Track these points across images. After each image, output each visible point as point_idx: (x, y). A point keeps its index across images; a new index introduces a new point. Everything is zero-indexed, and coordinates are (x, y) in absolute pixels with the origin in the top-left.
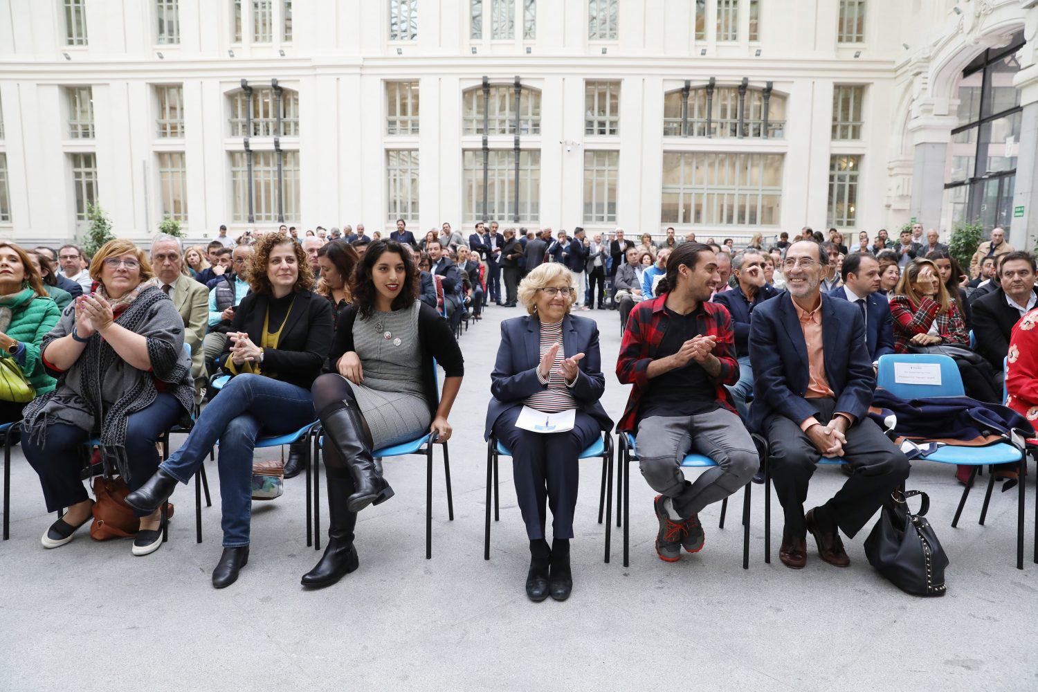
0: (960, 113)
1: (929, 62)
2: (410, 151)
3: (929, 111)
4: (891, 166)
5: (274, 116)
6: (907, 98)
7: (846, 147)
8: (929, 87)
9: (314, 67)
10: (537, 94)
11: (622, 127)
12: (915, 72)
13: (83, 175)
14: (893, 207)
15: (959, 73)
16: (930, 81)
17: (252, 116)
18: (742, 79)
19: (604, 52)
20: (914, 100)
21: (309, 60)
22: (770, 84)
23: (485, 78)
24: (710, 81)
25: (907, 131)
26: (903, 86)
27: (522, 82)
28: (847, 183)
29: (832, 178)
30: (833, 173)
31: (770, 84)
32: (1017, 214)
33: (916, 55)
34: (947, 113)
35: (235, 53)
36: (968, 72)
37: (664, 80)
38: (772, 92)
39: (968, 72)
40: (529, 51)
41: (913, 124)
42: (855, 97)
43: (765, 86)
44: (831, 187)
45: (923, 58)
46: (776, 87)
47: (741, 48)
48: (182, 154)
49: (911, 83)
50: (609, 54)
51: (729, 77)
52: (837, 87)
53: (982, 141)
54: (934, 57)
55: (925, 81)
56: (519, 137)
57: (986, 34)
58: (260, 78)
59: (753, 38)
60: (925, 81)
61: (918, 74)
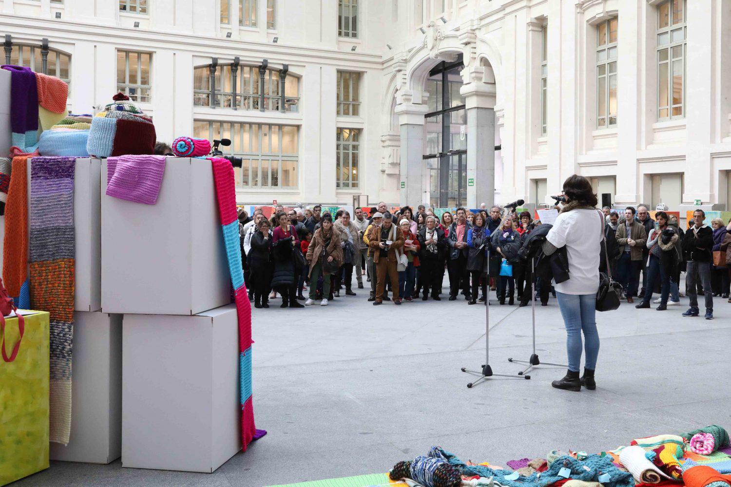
1: (406, 63)
3: (409, 100)
4: (384, 138)
7: (348, 122)
8: (408, 81)
12: (398, 69)
14: (386, 172)
15: (426, 73)
16: (408, 77)
19: (137, 25)
20: (397, 90)
22: (286, 67)
25: (393, 114)
26: (390, 76)
27: (51, 45)
28: (351, 151)
29: (338, 146)
30: (339, 143)
32: (470, 184)
33: (399, 54)
37: (193, 56)
39: (433, 72)
41: (398, 109)
42: (353, 84)
43: (281, 67)
44: (338, 153)
45: (402, 60)
46: (291, 69)
49: (394, 76)
50: (141, 27)
52: (340, 72)
53: (445, 125)
54: (410, 61)
55: (405, 77)
57: (441, 53)
60: (405, 77)
61: (400, 71)
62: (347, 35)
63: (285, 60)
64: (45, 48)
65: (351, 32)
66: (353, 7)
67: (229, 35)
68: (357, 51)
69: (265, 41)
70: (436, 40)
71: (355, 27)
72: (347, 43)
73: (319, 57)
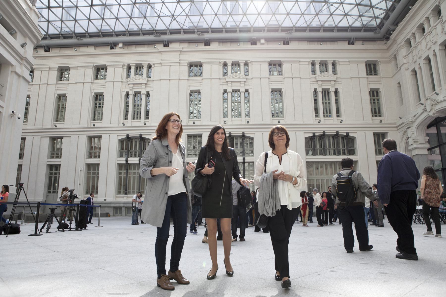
0: (429, 142)
5: (139, 149)
6: (405, 138)
10: (252, 139)
13: (53, 174)
17: (142, 149)
18: (336, 132)
20: (408, 138)
24: (323, 133)
26: (403, 132)
27: (245, 135)
31: (347, 134)
34: (424, 142)
36: (429, 127)
37: (304, 133)
38: (348, 137)
39: (429, 127)
47: (334, 120)
48: (98, 165)
49: (406, 131)
51: (331, 131)
52: (374, 134)
55: (413, 130)
58: (134, 134)
59: (338, 116)
60: (413, 130)
62: (376, 116)
63: (347, 130)
65: (378, 114)
66: (377, 103)
67: (319, 122)
68: (383, 122)
69: (336, 123)
70: (432, 105)
71: (379, 112)
72: (377, 119)
73: (364, 127)
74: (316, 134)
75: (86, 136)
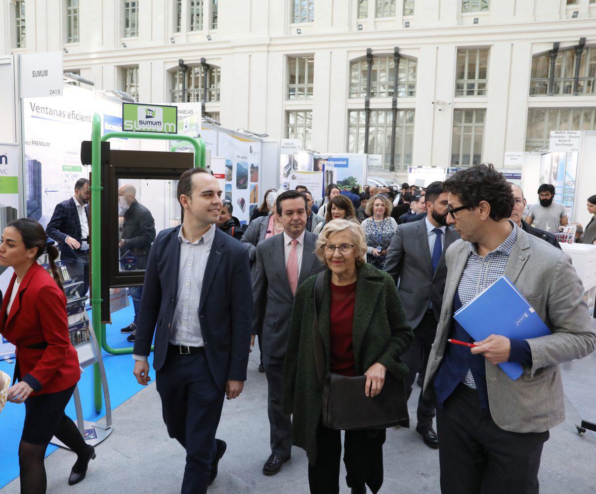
2: (305, 111)
5: (202, 87)
9: (233, 47)
10: (415, 60)
11: (490, 87)
19: (476, 21)
21: (229, 42)
23: (369, 50)
24: (580, 41)
27: (401, 52)
35: (176, 39)
40: (407, 25)
56: (396, 99)
58: (192, 58)
64: (397, 56)
74: (562, 46)
75: (115, 66)
